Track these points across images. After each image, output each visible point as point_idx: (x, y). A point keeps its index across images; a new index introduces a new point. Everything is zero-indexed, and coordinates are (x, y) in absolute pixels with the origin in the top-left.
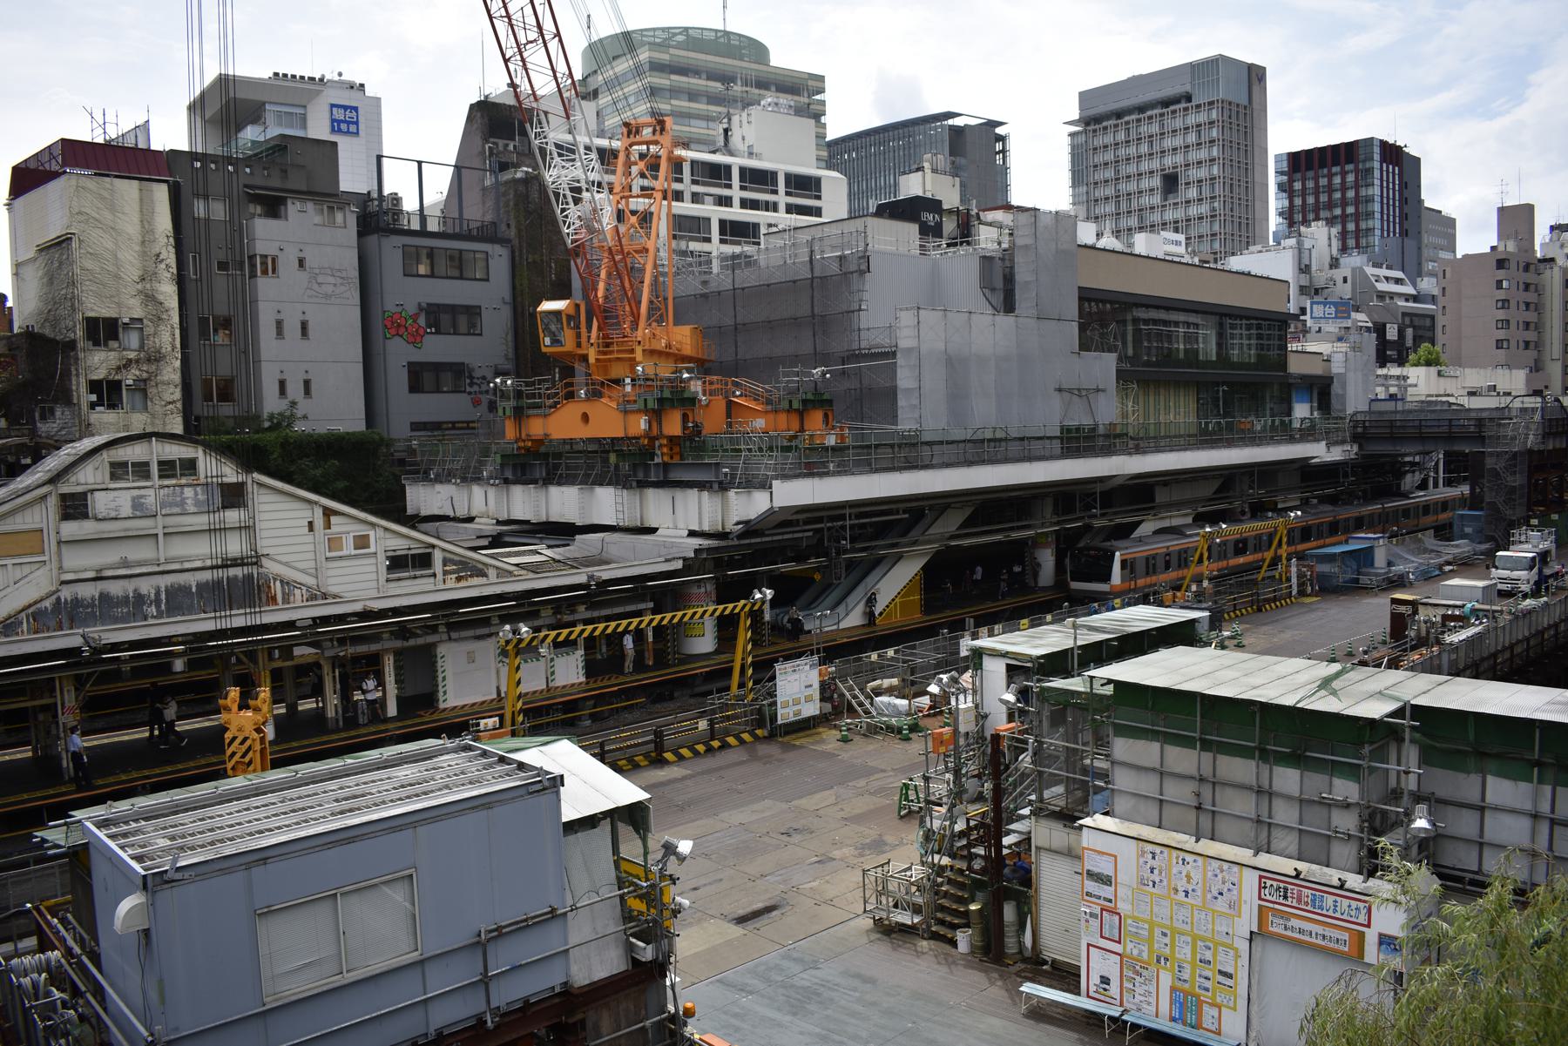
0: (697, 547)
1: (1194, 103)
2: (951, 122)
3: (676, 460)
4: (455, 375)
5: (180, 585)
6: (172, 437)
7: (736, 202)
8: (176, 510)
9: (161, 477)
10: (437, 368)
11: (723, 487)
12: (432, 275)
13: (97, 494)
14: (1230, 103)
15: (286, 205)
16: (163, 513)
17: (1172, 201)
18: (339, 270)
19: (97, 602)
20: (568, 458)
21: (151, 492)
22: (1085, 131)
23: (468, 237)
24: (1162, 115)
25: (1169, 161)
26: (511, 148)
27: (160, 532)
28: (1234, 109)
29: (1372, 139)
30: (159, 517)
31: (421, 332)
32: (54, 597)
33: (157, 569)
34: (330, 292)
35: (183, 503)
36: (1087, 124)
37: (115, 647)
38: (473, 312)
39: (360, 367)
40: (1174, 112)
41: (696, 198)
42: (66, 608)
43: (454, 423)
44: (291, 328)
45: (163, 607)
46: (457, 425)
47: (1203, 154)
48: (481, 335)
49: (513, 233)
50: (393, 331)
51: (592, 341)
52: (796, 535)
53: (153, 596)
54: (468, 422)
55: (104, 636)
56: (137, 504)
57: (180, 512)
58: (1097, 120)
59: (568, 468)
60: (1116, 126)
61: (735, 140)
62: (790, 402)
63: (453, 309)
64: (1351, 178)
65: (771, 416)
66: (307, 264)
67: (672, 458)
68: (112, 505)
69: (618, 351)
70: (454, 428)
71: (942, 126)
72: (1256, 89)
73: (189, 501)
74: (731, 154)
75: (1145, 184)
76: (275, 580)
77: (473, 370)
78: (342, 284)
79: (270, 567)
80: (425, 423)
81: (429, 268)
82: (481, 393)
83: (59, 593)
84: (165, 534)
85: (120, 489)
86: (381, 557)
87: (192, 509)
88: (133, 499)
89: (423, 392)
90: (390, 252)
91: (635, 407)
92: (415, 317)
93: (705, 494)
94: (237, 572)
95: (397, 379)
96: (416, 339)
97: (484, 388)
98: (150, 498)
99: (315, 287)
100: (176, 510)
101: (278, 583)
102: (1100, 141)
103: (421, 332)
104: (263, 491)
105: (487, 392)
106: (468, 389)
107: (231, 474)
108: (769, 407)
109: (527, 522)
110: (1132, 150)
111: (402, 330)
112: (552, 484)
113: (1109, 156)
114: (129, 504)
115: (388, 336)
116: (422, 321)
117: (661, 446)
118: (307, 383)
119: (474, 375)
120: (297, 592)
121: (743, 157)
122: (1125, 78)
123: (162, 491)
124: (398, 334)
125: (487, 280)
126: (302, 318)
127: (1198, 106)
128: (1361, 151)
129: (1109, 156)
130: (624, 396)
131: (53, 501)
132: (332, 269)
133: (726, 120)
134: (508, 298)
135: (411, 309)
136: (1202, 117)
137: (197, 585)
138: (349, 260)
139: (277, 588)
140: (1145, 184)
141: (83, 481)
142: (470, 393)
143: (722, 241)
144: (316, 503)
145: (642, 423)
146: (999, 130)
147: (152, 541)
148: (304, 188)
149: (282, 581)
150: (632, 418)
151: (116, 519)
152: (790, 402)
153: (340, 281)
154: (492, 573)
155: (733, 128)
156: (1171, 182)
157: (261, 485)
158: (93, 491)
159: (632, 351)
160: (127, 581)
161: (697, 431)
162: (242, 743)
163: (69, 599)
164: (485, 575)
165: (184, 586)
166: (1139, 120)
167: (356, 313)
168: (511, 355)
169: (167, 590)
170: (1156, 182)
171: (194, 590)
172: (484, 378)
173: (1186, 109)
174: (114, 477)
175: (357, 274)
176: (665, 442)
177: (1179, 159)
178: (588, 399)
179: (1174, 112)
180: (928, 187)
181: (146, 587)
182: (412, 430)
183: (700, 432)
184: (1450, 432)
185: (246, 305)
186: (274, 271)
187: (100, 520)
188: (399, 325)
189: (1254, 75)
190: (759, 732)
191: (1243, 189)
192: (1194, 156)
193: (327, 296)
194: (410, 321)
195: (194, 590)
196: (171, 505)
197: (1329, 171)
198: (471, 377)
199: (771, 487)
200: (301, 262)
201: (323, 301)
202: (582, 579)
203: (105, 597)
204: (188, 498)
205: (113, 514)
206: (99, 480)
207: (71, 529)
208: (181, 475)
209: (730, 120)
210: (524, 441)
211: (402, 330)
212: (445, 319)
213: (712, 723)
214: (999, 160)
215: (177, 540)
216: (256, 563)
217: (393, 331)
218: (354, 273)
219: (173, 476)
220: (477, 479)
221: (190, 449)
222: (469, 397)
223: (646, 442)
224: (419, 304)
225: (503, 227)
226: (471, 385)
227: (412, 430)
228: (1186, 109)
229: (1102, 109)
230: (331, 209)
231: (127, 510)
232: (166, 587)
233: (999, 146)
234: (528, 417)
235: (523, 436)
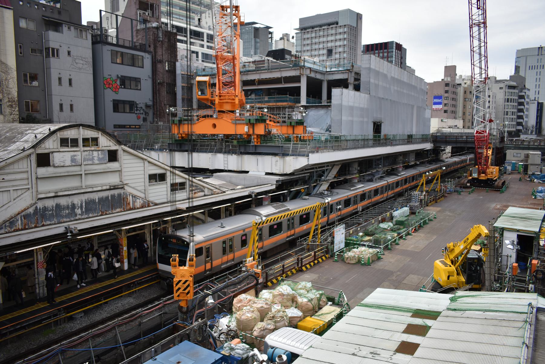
0: (278, 180)
1: (339, 25)
2: (254, 26)
3: (259, 144)
4: (132, 106)
5: (91, 199)
6: (89, 127)
7: (205, 46)
8: (90, 162)
9: (84, 146)
10: (124, 102)
11: (285, 155)
12: (122, 64)
13: (55, 154)
14: (351, 26)
15: (62, 27)
16: (84, 164)
17: (330, 59)
18: (84, 58)
19: (54, 208)
20: (201, 142)
21: (79, 153)
22: (301, 33)
23: (134, 48)
24: (328, 28)
25: (330, 45)
26: (147, 14)
27: (83, 173)
28: (352, 28)
29: (393, 42)
30: (83, 166)
31: (118, 87)
32: (35, 206)
33: (83, 191)
34: (81, 67)
35: (93, 159)
36: (302, 30)
37: (83, 232)
38: (137, 80)
39: (93, 99)
40: (332, 28)
41: (191, 43)
42: (40, 212)
43: (130, 126)
44: (65, 82)
45: (84, 210)
46: (131, 127)
47: (341, 43)
48: (140, 90)
49: (152, 49)
50: (107, 86)
51: (217, 94)
52: (303, 175)
53: (79, 205)
54: (135, 126)
55: (76, 226)
56: (73, 160)
57: (91, 163)
58: (305, 29)
59: (201, 146)
60: (312, 31)
61: (203, 23)
62: (291, 123)
63: (131, 79)
64: (386, 54)
65: (278, 128)
66: (72, 53)
67: (257, 143)
68: (62, 160)
69: (228, 99)
70: (130, 128)
71: (251, 27)
72: (359, 21)
73: (96, 158)
74: (201, 28)
75: (321, 52)
76: (129, 195)
77: (138, 104)
78: (86, 64)
79: (128, 189)
80: (119, 125)
81: (121, 60)
82: (140, 114)
83: (37, 205)
84: (85, 174)
85: (65, 151)
86: (169, 185)
87: (97, 162)
88: (72, 156)
89: (118, 112)
90: (106, 52)
91: (244, 122)
92: (116, 81)
93: (277, 158)
94: (116, 192)
95: (109, 106)
96: (116, 91)
97: (142, 112)
98: (79, 156)
100: (90, 162)
101: (131, 197)
102: (306, 36)
103: (118, 87)
104: (125, 154)
105: (142, 113)
106: (136, 112)
107: (114, 147)
108: (278, 124)
109: (183, 168)
110: (317, 40)
111: (111, 86)
112: (194, 152)
113: (309, 42)
114: (70, 159)
115: (105, 88)
116: (118, 83)
117: (254, 138)
118: (71, 106)
119: (139, 106)
120: (138, 200)
121: (206, 29)
122: (314, 15)
123: (84, 153)
124: (109, 87)
125: (143, 67)
126: (69, 77)
127: (340, 26)
128: (390, 45)
129: (309, 42)
130: (236, 117)
131: (34, 158)
132: (82, 57)
133: (199, 15)
134: (151, 76)
135: (114, 77)
136: (341, 30)
137: (99, 198)
138: (88, 54)
139: (130, 199)
140: (321, 52)
141: (48, 147)
142: (136, 114)
143: (203, 61)
144: (146, 160)
145: (246, 129)
146: (270, 30)
147: (79, 177)
148: (68, 20)
149: (132, 196)
150: (239, 127)
151: (63, 166)
152: (291, 123)
153: (85, 63)
154: (206, 192)
155: (202, 18)
156: (330, 52)
157: (124, 151)
158: (53, 152)
159: (234, 100)
160: (68, 197)
161: (270, 132)
162: (184, 283)
163: (41, 208)
164: (203, 191)
165: (93, 200)
166: (320, 30)
167: (91, 77)
168: (151, 98)
169: (85, 201)
170: (325, 52)
171: (97, 201)
172: (141, 108)
173: (336, 27)
174: (61, 146)
175: (92, 60)
176: (256, 136)
178: (217, 118)
179: (332, 28)
180: (286, 46)
181: (77, 200)
182: (114, 128)
183: (270, 133)
184: (467, 140)
185: (46, 70)
186: (57, 56)
187: (56, 167)
188: (110, 84)
189: (359, 17)
190: (327, 256)
191: (354, 56)
192: (338, 43)
193: (80, 69)
194: (114, 82)
195: (97, 201)
196: (88, 160)
197: (383, 51)
198: (137, 107)
199: (308, 156)
200: (69, 53)
201: (78, 70)
202: (246, 193)
203: (58, 206)
204: (95, 157)
205: (62, 164)
206: (55, 147)
207: (43, 171)
208: (92, 145)
209: (201, 15)
210: (181, 134)
211: (111, 86)
212: (127, 82)
213: (315, 253)
214: (270, 40)
215: (90, 177)
216: (122, 188)
217: (107, 86)
218: (90, 60)
219: (89, 146)
220: (152, 149)
221: (96, 133)
222: (136, 115)
223: (246, 136)
224: (118, 75)
225: (147, 46)
226: (137, 110)
227: (114, 128)
228: (336, 27)
229: (307, 25)
230: (81, 31)
231: (68, 163)
232: (86, 200)
233: (270, 36)
234: (184, 124)
235: (181, 132)
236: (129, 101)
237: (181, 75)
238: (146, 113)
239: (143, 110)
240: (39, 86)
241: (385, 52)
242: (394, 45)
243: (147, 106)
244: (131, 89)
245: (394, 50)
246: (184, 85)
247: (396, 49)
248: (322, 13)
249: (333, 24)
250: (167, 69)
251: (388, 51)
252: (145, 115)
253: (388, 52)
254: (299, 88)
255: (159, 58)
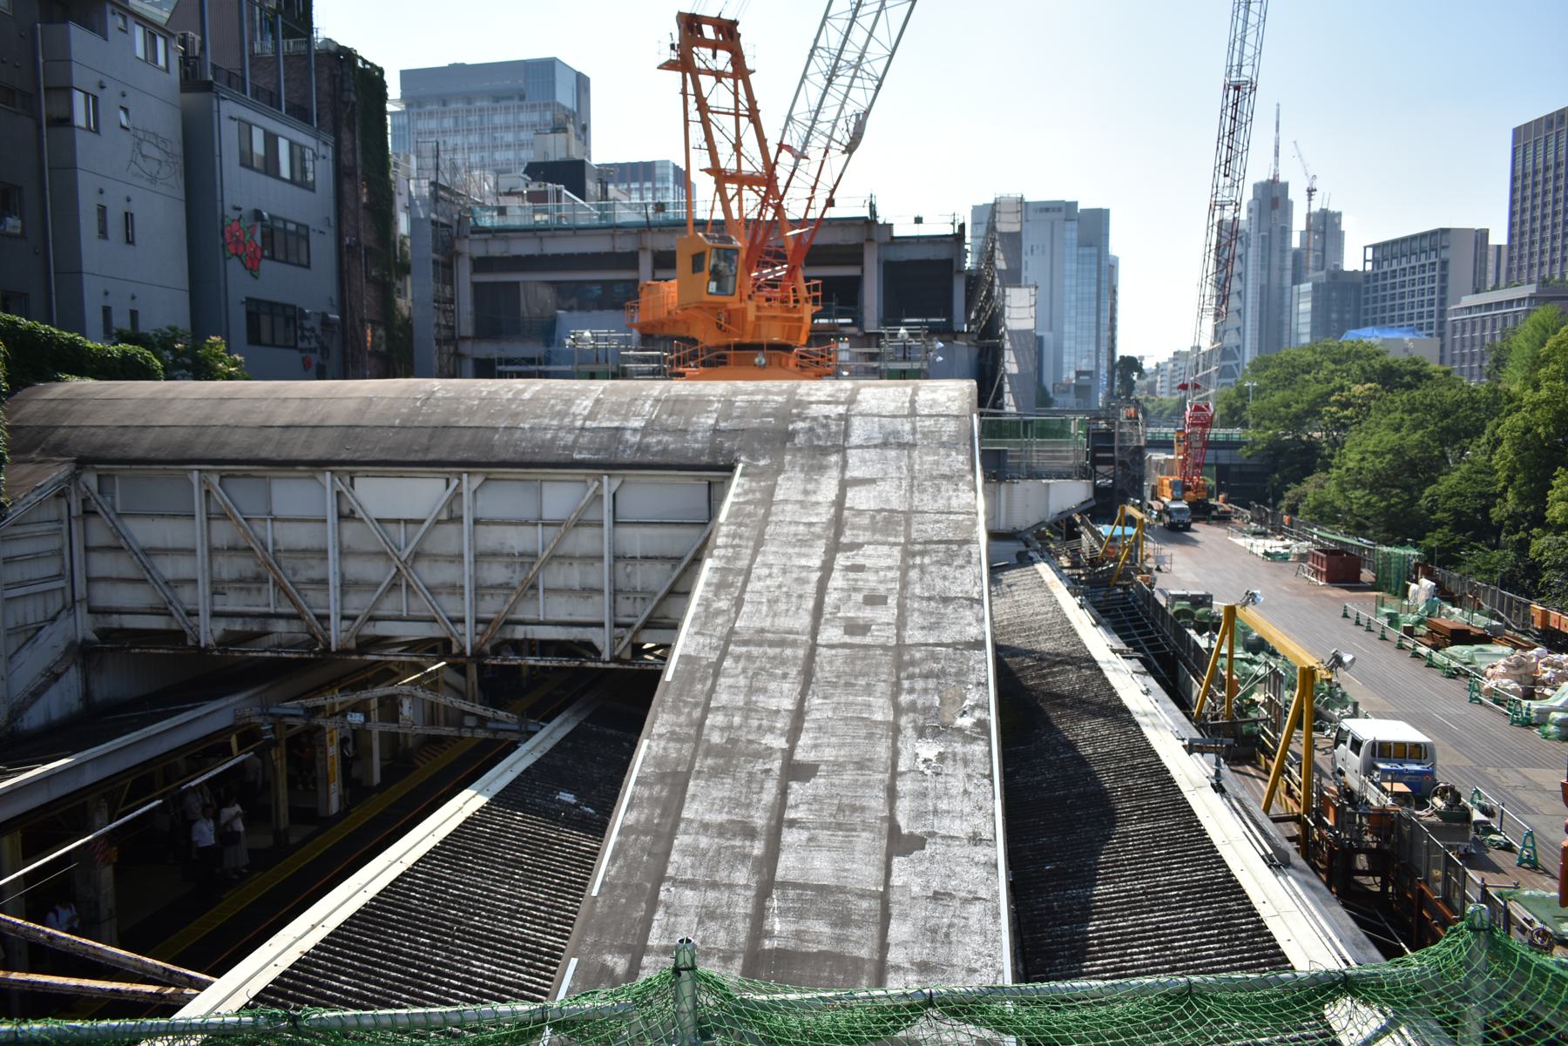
1: (527, 102)
29: (668, 161)
39: (187, 294)
48: (308, 266)
72: (582, 96)
97: (314, 344)
99: (140, 160)
103: (259, 254)
105: (313, 351)
119: (307, 324)
122: (445, 64)
124: (236, 254)
128: (658, 171)
132: (156, 136)
142: (301, 350)
172: (312, 330)
177: (511, 155)
197: (654, 185)
226: (303, 338)
228: (520, 107)
236: (284, 306)
237: (429, 228)
238: (325, 351)
239: (317, 337)
240: (23, 236)
241: (648, 189)
242: (671, 172)
243: (325, 322)
244: (286, 262)
245: (671, 185)
246: (435, 256)
247: (676, 182)
248: (468, 62)
249: (510, 98)
250: (365, 199)
251: (654, 185)
252: (322, 354)
253: (655, 190)
254: (856, 283)
255: (346, 159)
